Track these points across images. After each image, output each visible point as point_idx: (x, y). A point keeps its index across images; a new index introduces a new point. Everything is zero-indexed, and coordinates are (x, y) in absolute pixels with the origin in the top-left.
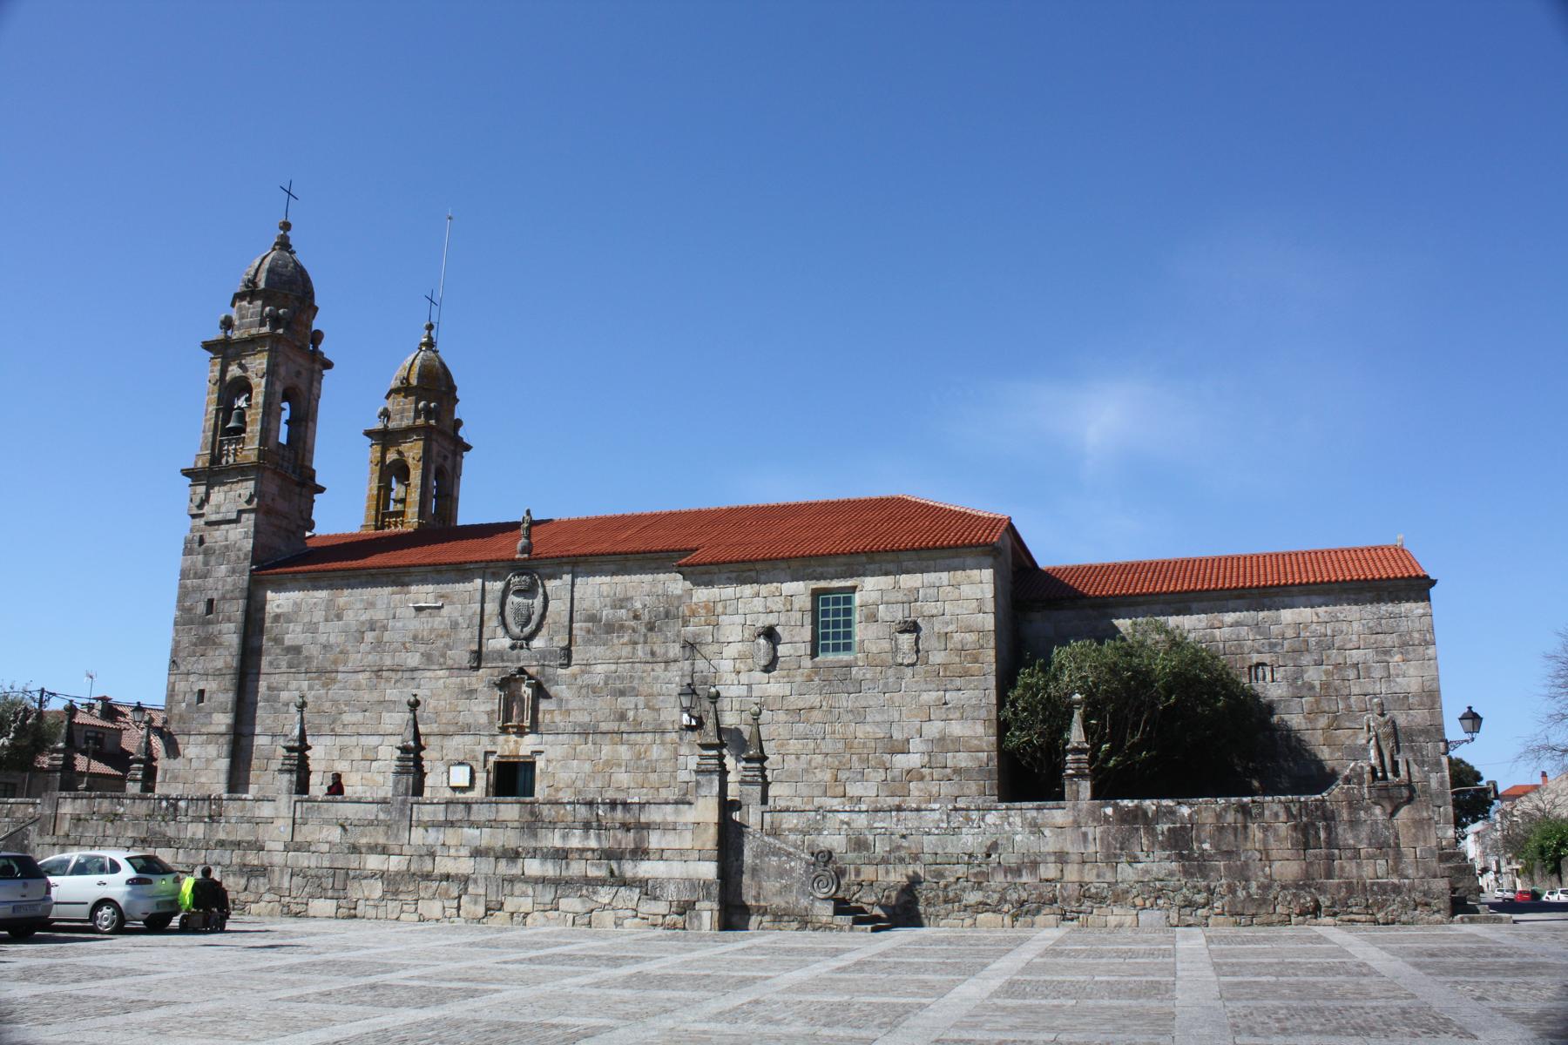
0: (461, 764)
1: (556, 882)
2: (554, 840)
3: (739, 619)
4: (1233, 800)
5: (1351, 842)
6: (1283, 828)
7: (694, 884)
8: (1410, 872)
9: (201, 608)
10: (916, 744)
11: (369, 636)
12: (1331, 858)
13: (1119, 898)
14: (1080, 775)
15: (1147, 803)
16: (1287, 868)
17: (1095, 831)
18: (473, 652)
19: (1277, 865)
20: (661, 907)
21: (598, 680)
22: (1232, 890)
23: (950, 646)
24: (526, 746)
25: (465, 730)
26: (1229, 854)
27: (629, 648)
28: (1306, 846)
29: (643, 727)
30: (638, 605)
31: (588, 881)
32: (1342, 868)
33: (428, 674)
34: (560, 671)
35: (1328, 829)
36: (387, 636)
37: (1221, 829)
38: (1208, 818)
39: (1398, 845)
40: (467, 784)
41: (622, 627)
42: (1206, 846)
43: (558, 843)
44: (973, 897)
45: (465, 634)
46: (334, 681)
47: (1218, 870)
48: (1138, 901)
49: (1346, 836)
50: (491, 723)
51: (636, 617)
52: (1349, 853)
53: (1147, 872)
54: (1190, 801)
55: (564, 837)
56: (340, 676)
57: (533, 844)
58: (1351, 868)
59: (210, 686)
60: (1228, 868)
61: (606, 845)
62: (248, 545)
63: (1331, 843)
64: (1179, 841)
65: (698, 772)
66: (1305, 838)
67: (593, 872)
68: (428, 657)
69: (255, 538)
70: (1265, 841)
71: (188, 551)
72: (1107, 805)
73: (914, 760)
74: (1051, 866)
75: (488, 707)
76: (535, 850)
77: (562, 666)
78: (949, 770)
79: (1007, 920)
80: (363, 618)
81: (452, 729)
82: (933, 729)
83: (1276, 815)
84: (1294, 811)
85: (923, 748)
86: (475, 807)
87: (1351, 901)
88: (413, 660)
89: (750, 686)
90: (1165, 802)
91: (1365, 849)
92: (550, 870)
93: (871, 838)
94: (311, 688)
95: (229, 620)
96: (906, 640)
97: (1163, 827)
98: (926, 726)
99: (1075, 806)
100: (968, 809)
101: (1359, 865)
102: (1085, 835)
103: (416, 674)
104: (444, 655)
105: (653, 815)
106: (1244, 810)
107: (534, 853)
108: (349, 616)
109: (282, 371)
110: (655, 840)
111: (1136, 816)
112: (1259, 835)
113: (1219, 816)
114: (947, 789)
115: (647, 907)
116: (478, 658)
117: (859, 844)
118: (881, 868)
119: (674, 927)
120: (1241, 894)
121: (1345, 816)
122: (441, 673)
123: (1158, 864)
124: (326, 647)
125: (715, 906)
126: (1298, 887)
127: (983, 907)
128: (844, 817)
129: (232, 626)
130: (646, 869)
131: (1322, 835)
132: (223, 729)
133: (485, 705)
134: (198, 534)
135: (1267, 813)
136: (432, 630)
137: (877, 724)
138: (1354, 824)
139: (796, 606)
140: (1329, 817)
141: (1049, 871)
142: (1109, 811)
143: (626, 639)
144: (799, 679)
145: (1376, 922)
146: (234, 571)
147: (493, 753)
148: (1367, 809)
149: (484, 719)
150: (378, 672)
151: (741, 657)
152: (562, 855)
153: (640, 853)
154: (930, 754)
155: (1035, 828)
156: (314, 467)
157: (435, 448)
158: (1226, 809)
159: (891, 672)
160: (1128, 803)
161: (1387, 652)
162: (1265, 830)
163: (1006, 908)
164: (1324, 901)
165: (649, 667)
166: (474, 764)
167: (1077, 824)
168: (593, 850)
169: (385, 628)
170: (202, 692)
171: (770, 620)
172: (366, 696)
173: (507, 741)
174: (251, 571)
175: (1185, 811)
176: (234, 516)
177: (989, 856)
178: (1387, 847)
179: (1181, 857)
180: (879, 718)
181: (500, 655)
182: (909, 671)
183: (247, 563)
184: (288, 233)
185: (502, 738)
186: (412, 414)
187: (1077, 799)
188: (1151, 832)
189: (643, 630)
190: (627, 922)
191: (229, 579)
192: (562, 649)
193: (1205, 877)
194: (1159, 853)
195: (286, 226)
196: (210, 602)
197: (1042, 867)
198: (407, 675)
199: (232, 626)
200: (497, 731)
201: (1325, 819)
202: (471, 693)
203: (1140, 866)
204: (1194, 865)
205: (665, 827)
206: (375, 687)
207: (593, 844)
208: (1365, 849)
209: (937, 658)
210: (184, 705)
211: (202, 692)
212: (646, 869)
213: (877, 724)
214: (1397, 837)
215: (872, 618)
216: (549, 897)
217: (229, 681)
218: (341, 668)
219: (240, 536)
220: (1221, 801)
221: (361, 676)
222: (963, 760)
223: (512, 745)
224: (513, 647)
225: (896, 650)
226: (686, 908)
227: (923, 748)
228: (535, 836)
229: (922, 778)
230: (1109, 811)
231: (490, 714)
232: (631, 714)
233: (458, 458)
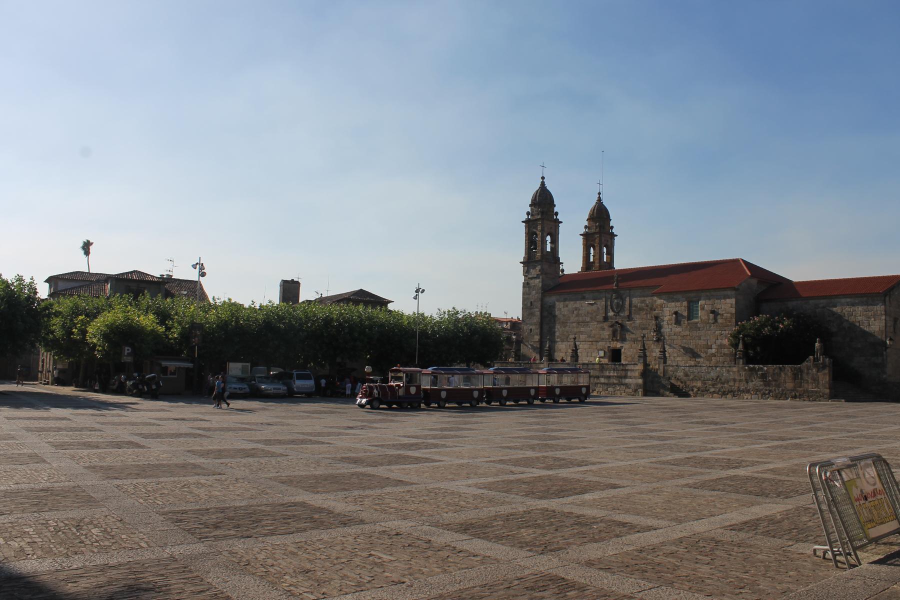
0: (601, 350)
1: (607, 384)
2: (607, 374)
3: (668, 309)
4: (778, 366)
5: (807, 379)
6: (789, 374)
7: (637, 385)
8: (821, 387)
9: (529, 304)
10: (714, 346)
11: (575, 312)
12: (801, 383)
13: (748, 391)
14: (740, 358)
15: (756, 366)
16: (790, 385)
17: (743, 373)
18: (604, 317)
19: (787, 384)
20: (630, 390)
21: (638, 325)
22: (775, 390)
23: (723, 318)
24: (619, 345)
25: (603, 340)
26: (775, 381)
27: (645, 316)
28: (795, 380)
29: (650, 339)
30: (648, 302)
31: (614, 384)
32: (804, 385)
33: (592, 323)
34: (627, 322)
35: (801, 375)
36: (580, 312)
37: (774, 374)
38: (771, 371)
39: (818, 380)
40: (603, 356)
41: (644, 309)
42: (770, 378)
43: (608, 374)
44: (712, 390)
45: (601, 312)
46: (567, 325)
47: (772, 385)
48: (752, 392)
49: (805, 376)
50: (609, 338)
51: (647, 306)
52: (805, 382)
53: (755, 384)
54: (767, 366)
55: (609, 373)
56: (568, 324)
57: (602, 374)
58: (806, 386)
59: (533, 327)
60: (775, 384)
61: (619, 375)
62: (540, 285)
63: (801, 379)
64: (764, 376)
65: (638, 357)
66: (795, 377)
67: (615, 382)
68: (591, 318)
69: (542, 282)
70: (785, 378)
71: (524, 287)
72: (746, 366)
73: (713, 351)
74: (732, 382)
75: (608, 333)
76: (603, 376)
77: (628, 321)
78: (722, 354)
79: (720, 396)
80: (574, 307)
81: (599, 340)
82: (718, 342)
83: (788, 371)
84: (793, 370)
85: (716, 347)
86: (589, 365)
87: (805, 395)
88: (588, 319)
89: (671, 329)
90: (761, 366)
91: (810, 381)
92: (606, 381)
93: (689, 373)
94: (561, 328)
95: (536, 308)
96: (711, 316)
97: (760, 373)
98: (717, 341)
99: (738, 366)
100: (712, 366)
101: (808, 385)
102: (740, 374)
103: (589, 324)
104: (596, 318)
105: (629, 367)
106: (780, 368)
107: (602, 377)
108: (570, 306)
109: (546, 229)
110: (629, 374)
111: (754, 369)
112: (783, 376)
113: (774, 370)
114: (721, 359)
115: (627, 390)
116: (606, 319)
117: (686, 375)
118: (691, 382)
119: (633, 395)
120: (777, 391)
121: (806, 371)
122: (595, 323)
123: (757, 383)
124: (564, 316)
125: (642, 390)
126: (792, 390)
127: (714, 392)
128: (682, 368)
129: (538, 310)
130: (627, 381)
131: (799, 376)
132: (537, 340)
133: (607, 333)
134: (526, 281)
135: (786, 370)
136: (592, 310)
137: (704, 340)
138: (808, 374)
139: (683, 305)
140: (801, 371)
141: (731, 383)
142: (747, 368)
143: (644, 313)
144: (684, 327)
145: (810, 401)
146: (537, 293)
147: (610, 347)
148: (812, 370)
149: (607, 337)
150: (578, 323)
151: (670, 320)
152: (609, 377)
153: (626, 377)
154: (717, 349)
155: (728, 371)
156: (559, 256)
157: (603, 239)
158: (775, 368)
159: (708, 325)
160: (751, 366)
161: (869, 318)
162: (785, 374)
163: (720, 393)
164: (798, 394)
165: (651, 321)
166: (605, 350)
167: (738, 371)
168: (616, 376)
169: (579, 310)
170: (531, 329)
171: (677, 309)
172: (575, 330)
173: (614, 343)
174: (542, 293)
175: (765, 368)
176: (536, 276)
177: (717, 379)
178: (815, 380)
179: (763, 381)
180: (705, 339)
181: (611, 318)
182: (713, 325)
183: (540, 291)
184: (544, 180)
185: (612, 342)
186: (595, 227)
187: (739, 364)
188: (757, 374)
189: (649, 310)
190: (623, 394)
191: (536, 295)
192: (628, 316)
193: (769, 386)
194: (758, 380)
195: (543, 178)
196: (531, 303)
197: (730, 383)
198: (586, 324)
199: (538, 310)
200: (610, 340)
201: (800, 372)
202: (603, 329)
203: (754, 383)
204: (767, 384)
205: (632, 370)
206: (578, 327)
207: (616, 375)
208: (810, 381)
209: (720, 321)
210: (526, 333)
211: (531, 329)
212: (627, 381)
213: (704, 340)
214: (818, 377)
215: (703, 309)
216: (606, 387)
217: (538, 326)
218: (568, 322)
219: (537, 282)
220: (775, 366)
221: (574, 324)
222: (726, 351)
223: (615, 344)
224: (614, 315)
225: (709, 319)
226: (636, 391)
227: (716, 347)
228: (603, 372)
229: (715, 356)
230: (747, 368)
231: (609, 335)
232: (646, 335)
233: (613, 240)
